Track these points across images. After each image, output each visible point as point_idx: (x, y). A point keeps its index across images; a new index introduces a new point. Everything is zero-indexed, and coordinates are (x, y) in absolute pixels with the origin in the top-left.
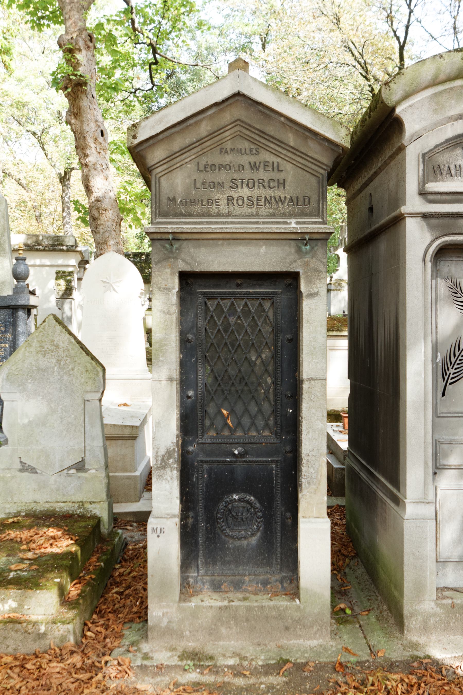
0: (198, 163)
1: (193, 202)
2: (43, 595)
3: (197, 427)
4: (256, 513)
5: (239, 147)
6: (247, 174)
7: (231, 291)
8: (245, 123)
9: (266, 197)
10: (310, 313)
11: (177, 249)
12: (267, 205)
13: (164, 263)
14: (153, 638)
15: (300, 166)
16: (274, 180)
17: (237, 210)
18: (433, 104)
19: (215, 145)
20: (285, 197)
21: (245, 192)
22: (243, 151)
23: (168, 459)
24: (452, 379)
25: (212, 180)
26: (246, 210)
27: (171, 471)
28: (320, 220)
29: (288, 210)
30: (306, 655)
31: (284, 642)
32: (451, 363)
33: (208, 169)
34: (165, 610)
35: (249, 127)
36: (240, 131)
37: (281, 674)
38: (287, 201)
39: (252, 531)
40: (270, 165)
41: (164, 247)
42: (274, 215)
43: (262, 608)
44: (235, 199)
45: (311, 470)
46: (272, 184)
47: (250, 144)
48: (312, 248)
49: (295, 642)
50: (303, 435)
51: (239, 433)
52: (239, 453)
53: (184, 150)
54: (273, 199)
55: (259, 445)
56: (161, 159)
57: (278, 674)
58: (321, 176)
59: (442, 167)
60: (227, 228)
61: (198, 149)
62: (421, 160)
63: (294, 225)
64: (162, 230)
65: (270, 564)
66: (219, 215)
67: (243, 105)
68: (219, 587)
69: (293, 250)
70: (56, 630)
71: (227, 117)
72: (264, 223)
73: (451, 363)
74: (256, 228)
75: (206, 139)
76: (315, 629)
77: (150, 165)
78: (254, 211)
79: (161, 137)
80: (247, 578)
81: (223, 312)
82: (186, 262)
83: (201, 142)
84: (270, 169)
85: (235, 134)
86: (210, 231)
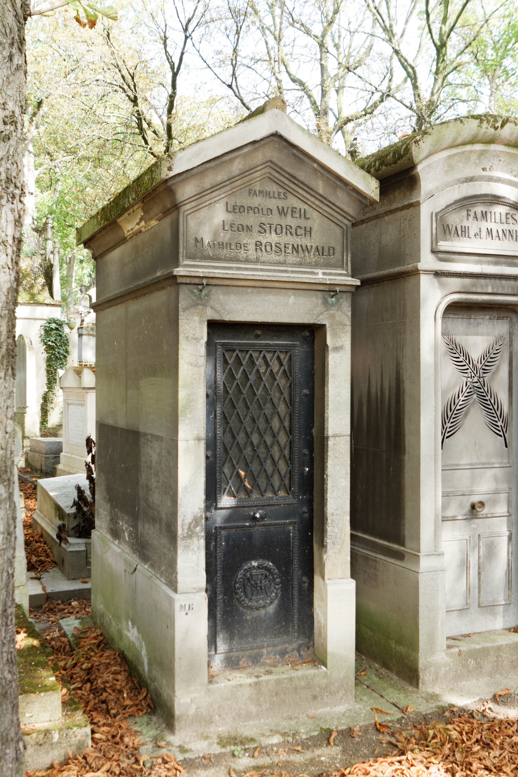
0: (227, 203)
1: (221, 245)
2: (48, 698)
3: (216, 491)
4: (274, 579)
5: (268, 190)
6: (275, 219)
7: (250, 342)
8: (276, 165)
9: (293, 245)
10: (335, 367)
11: (206, 295)
12: (294, 252)
13: (192, 310)
14: (181, 728)
15: (326, 215)
16: (301, 228)
17: (265, 256)
18: (446, 165)
19: (245, 185)
20: (312, 246)
21: (273, 238)
22: (272, 194)
23: (195, 527)
24: (448, 432)
25: (241, 223)
26: (274, 257)
27: (198, 540)
28: (345, 272)
29: (314, 260)
30: (343, 722)
31: (312, 712)
32: (448, 417)
33: (237, 211)
34: (193, 695)
35: (280, 170)
36: (270, 173)
37: (332, 744)
38: (313, 250)
39: (272, 599)
40: (298, 211)
41: (192, 292)
42: (300, 264)
43: (291, 679)
44: (264, 244)
45: (336, 530)
46: (299, 232)
47: (279, 187)
48: (338, 300)
49: (323, 710)
50: (328, 493)
51: (255, 495)
52: (261, 516)
53: (215, 188)
54: (300, 248)
55: (276, 507)
56: (192, 195)
57: (329, 743)
58: (345, 227)
59: (450, 227)
60: (259, 275)
61: (228, 188)
62: (434, 218)
63: (320, 276)
64: (193, 274)
65: (286, 633)
66: (247, 261)
67: (277, 146)
68: (237, 664)
69: (320, 302)
70: (73, 736)
71: (259, 157)
72: (293, 272)
73: (448, 417)
74: (288, 277)
75: (237, 178)
76: (341, 693)
77: (179, 202)
78: (281, 258)
79: (195, 171)
80: (264, 651)
81: (242, 365)
82: (215, 310)
83: (232, 181)
84: (298, 216)
85: (265, 176)
86: (243, 277)
